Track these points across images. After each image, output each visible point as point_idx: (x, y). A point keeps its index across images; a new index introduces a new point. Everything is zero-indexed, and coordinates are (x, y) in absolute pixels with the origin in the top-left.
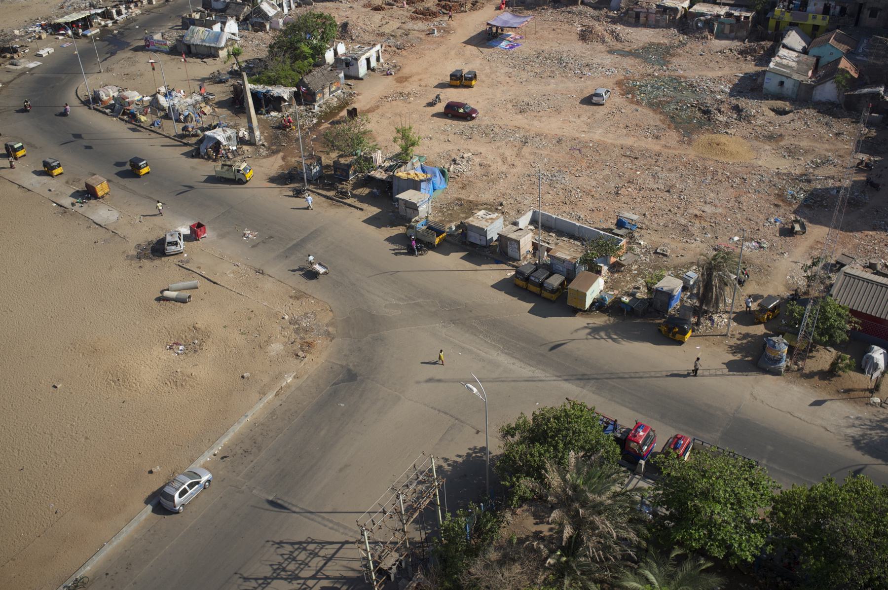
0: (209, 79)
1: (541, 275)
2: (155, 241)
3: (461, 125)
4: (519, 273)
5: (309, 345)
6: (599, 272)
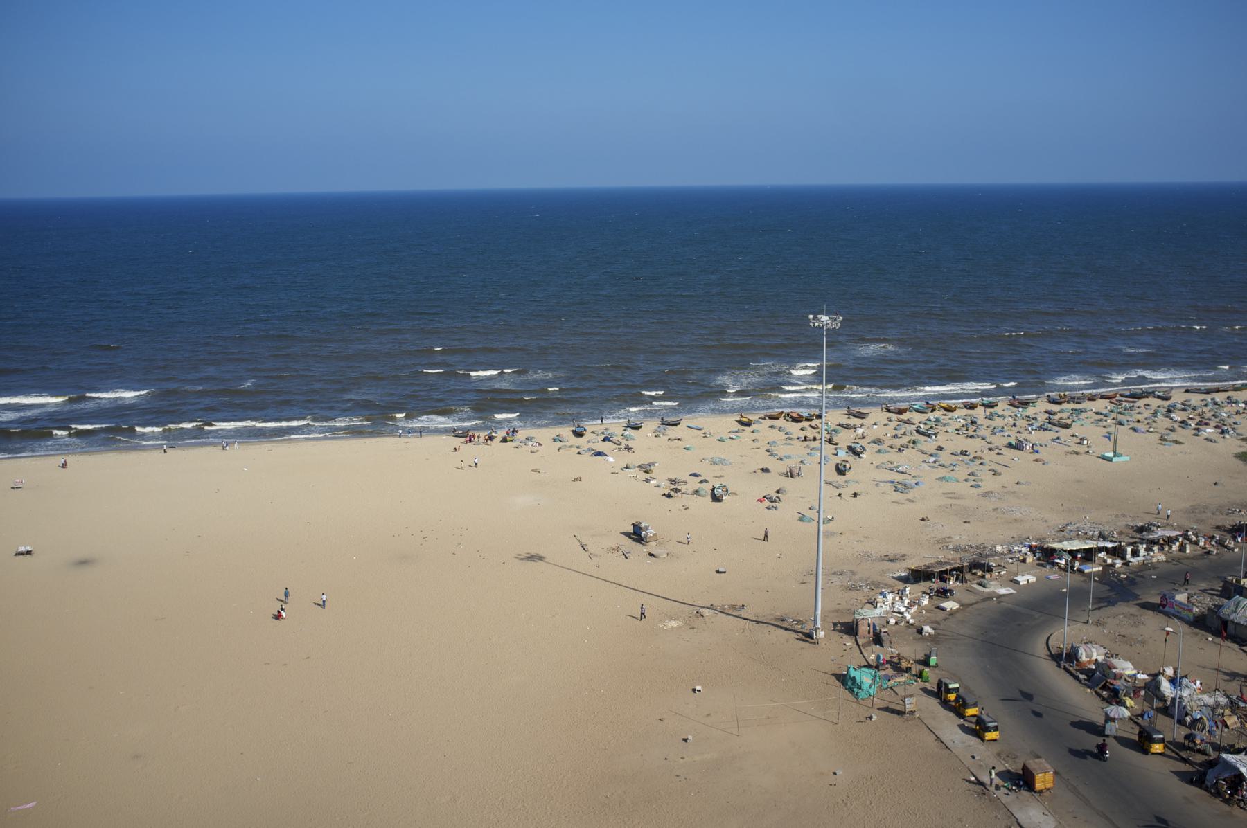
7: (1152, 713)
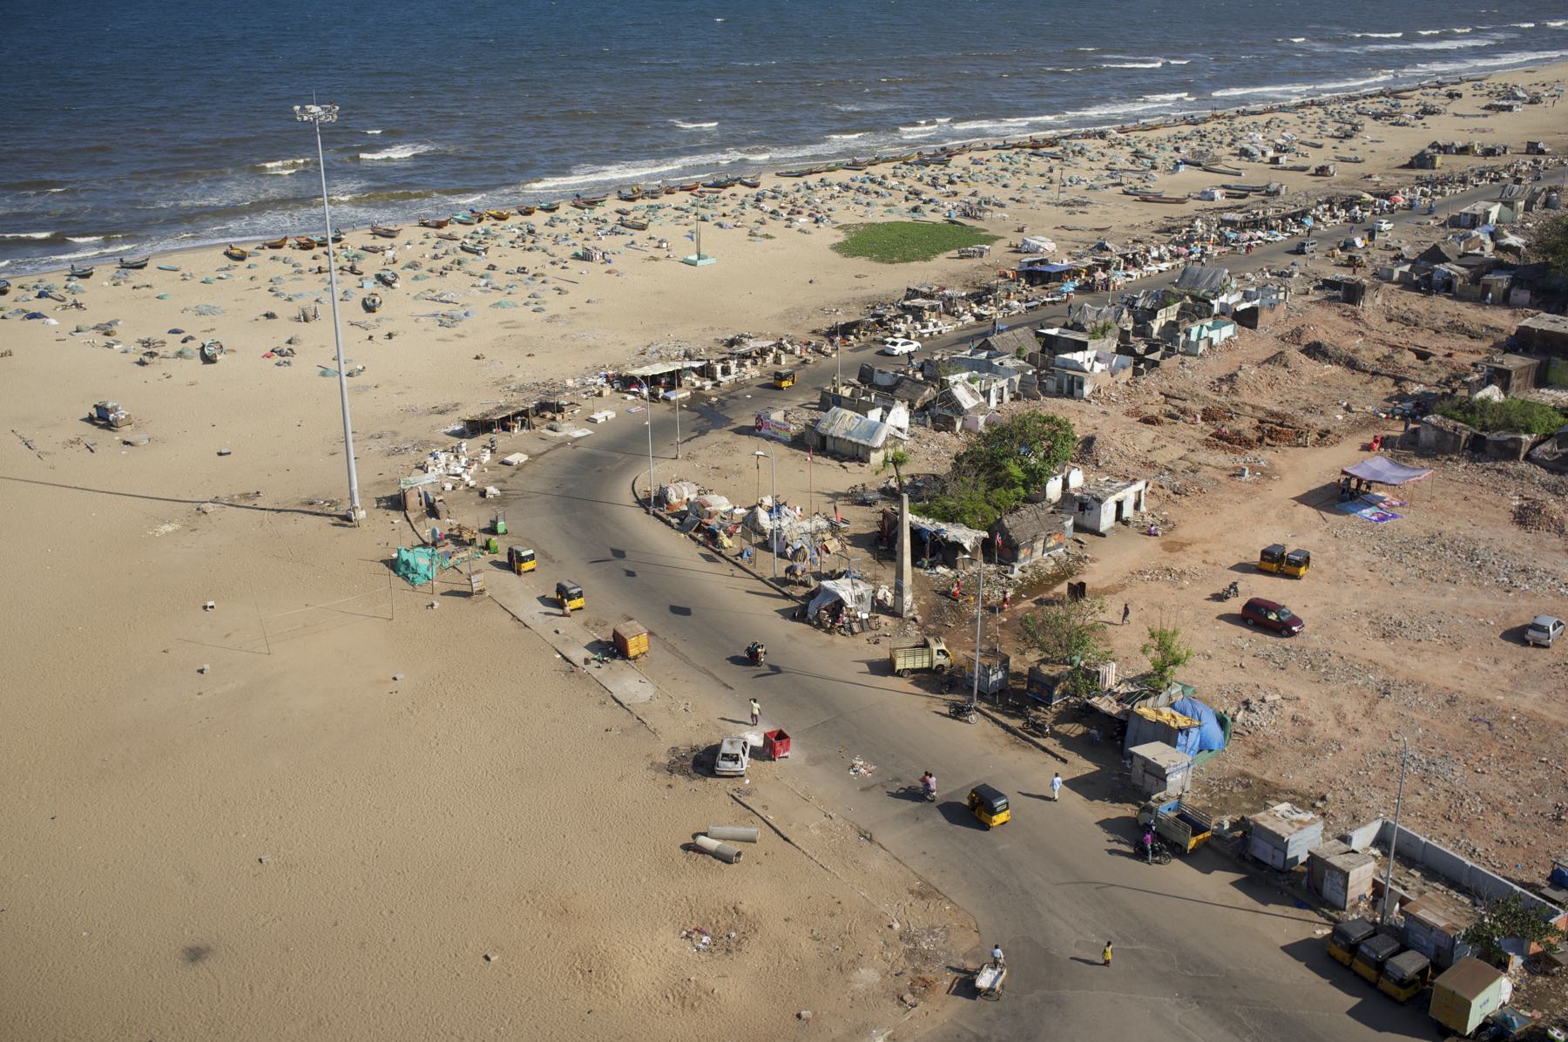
0: (846, 495)
1: (1381, 948)
2: (702, 746)
3: (1269, 642)
4: (1339, 933)
5: (927, 985)
6: (1503, 966)
7: (751, 550)
